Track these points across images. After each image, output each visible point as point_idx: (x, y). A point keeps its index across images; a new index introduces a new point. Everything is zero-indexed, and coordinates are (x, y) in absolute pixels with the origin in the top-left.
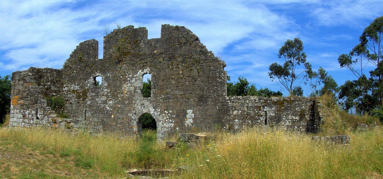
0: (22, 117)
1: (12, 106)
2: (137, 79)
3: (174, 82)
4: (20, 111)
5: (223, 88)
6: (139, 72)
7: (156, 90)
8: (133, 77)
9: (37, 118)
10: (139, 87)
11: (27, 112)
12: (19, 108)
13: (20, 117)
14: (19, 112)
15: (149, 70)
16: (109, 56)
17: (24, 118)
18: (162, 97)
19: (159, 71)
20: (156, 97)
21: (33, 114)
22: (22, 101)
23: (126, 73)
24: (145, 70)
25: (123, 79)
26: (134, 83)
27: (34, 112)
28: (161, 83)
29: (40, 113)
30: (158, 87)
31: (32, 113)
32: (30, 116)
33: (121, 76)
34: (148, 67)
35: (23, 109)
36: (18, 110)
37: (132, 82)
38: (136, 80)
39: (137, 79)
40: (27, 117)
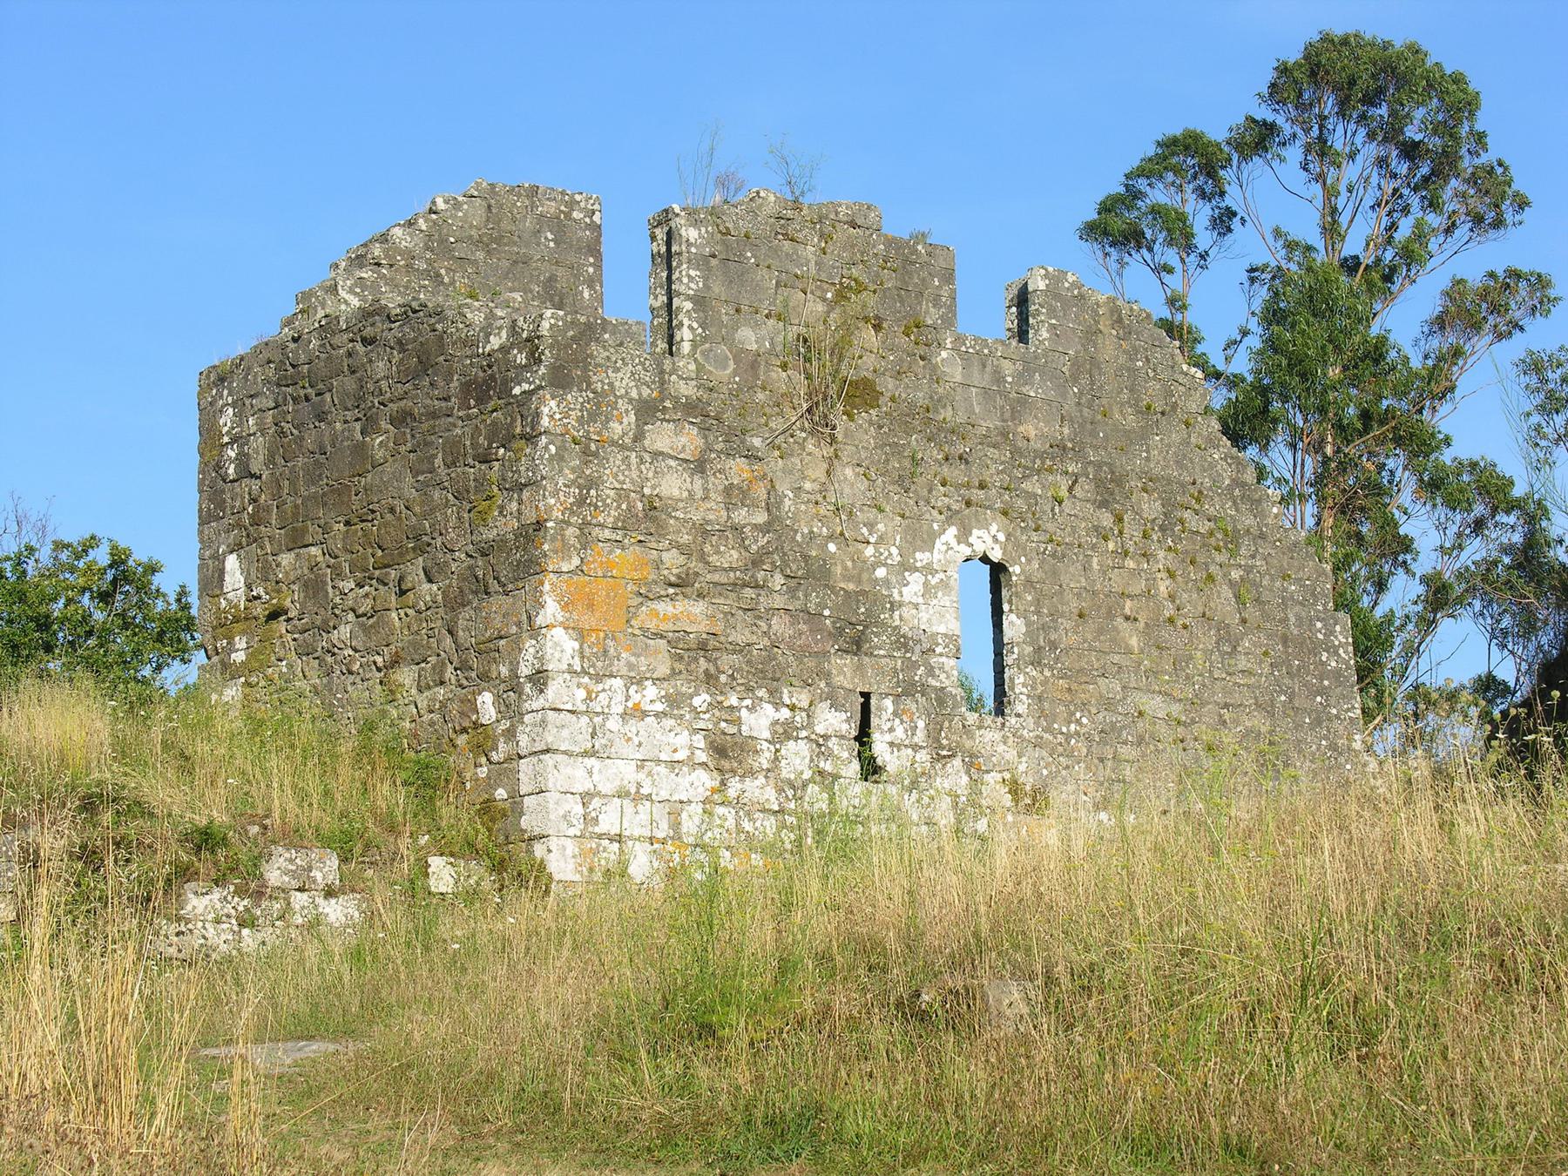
0: (702, 757)
1: (560, 647)
2: (934, 581)
3: (1134, 642)
4: (674, 701)
5: (1348, 710)
6: (944, 538)
7: (1047, 673)
8: (906, 567)
9: (871, 769)
10: (946, 635)
11: (759, 721)
12: (663, 670)
13: (682, 755)
14: (659, 707)
15: (1001, 537)
16: (735, 373)
17: (726, 764)
18: (1078, 722)
19: (1053, 555)
20: (1043, 715)
21: (826, 737)
22: (692, 615)
23: (864, 531)
24: (975, 532)
25: (845, 568)
26: (916, 606)
27: (836, 722)
28: (1068, 634)
29: (900, 732)
30: (1057, 660)
31: (820, 729)
32: (797, 757)
33: (831, 537)
34: (994, 519)
35: (710, 679)
36: (651, 691)
37: (901, 593)
38: (928, 591)
39: (934, 581)
40: (764, 760)
